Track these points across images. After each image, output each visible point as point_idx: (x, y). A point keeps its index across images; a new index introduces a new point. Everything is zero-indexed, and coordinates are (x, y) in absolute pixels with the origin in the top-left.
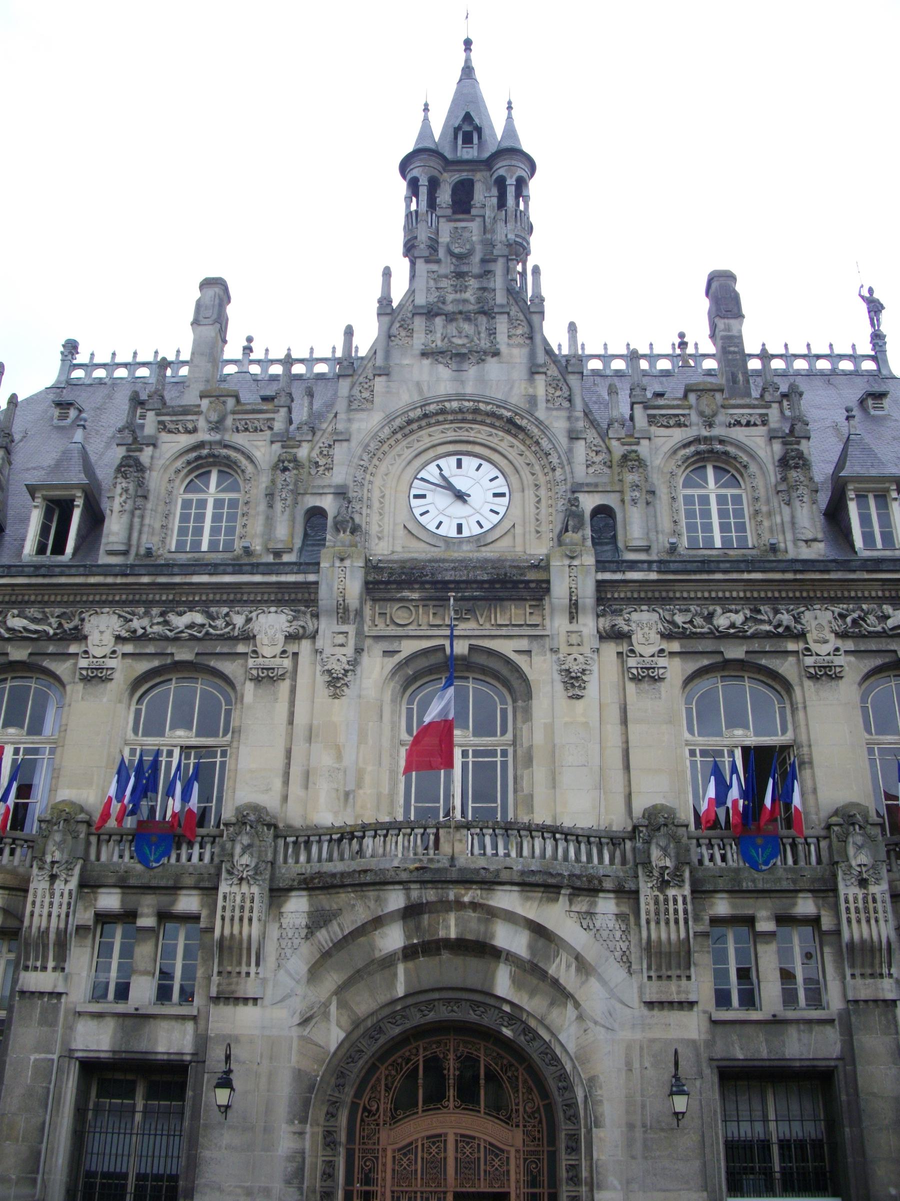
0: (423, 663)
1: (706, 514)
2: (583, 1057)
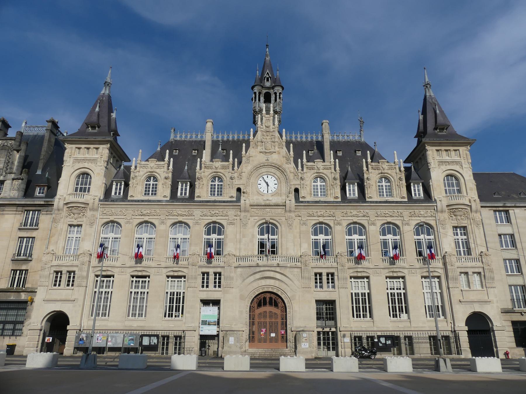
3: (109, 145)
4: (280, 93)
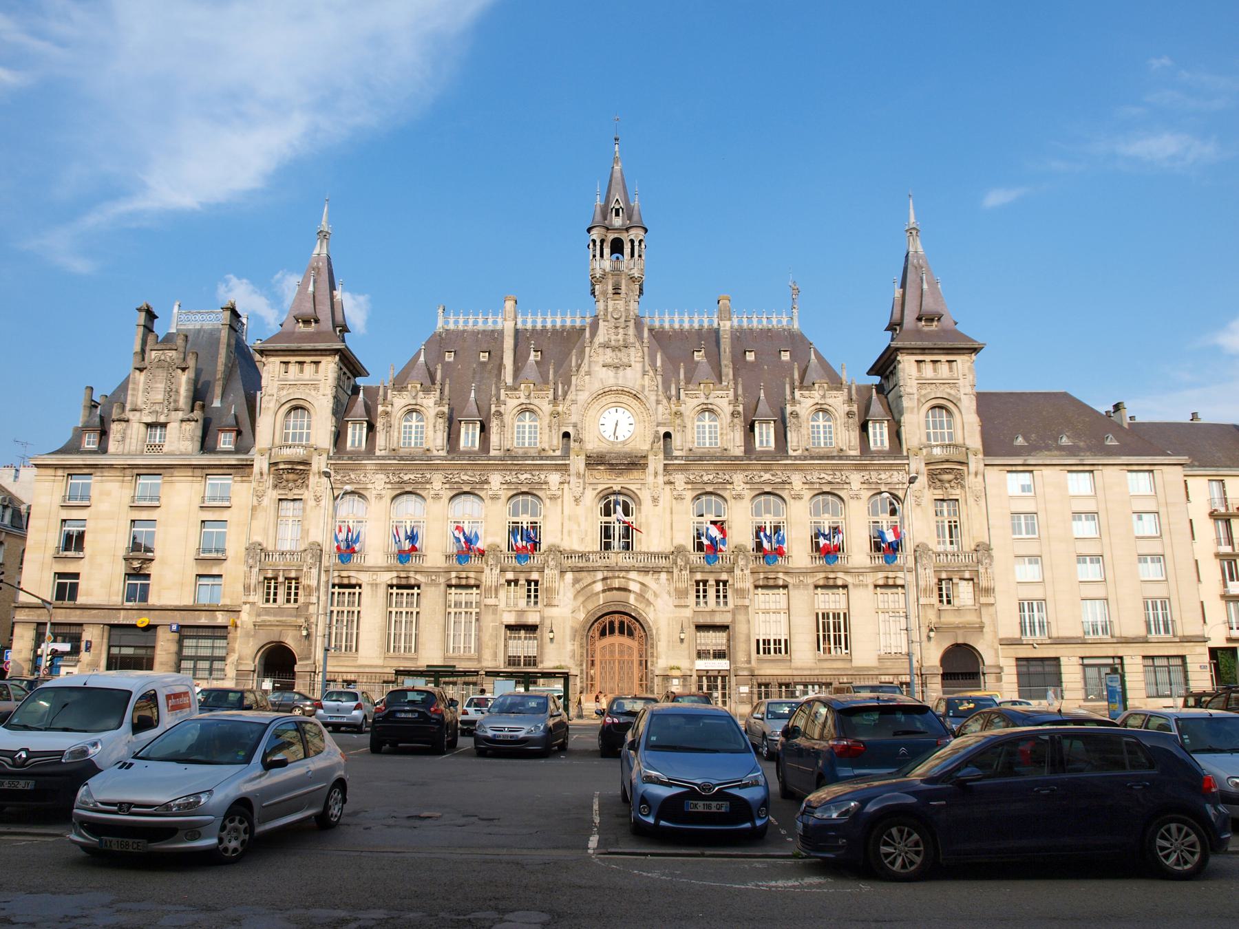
0: (606, 492)
1: (704, 432)
2: (655, 622)
3: (337, 358)
4: (640, 241)
